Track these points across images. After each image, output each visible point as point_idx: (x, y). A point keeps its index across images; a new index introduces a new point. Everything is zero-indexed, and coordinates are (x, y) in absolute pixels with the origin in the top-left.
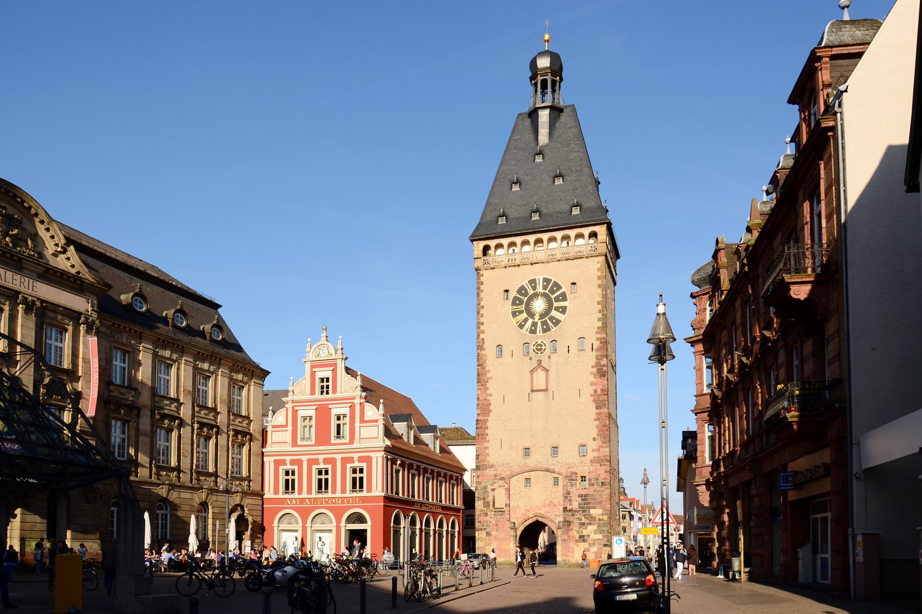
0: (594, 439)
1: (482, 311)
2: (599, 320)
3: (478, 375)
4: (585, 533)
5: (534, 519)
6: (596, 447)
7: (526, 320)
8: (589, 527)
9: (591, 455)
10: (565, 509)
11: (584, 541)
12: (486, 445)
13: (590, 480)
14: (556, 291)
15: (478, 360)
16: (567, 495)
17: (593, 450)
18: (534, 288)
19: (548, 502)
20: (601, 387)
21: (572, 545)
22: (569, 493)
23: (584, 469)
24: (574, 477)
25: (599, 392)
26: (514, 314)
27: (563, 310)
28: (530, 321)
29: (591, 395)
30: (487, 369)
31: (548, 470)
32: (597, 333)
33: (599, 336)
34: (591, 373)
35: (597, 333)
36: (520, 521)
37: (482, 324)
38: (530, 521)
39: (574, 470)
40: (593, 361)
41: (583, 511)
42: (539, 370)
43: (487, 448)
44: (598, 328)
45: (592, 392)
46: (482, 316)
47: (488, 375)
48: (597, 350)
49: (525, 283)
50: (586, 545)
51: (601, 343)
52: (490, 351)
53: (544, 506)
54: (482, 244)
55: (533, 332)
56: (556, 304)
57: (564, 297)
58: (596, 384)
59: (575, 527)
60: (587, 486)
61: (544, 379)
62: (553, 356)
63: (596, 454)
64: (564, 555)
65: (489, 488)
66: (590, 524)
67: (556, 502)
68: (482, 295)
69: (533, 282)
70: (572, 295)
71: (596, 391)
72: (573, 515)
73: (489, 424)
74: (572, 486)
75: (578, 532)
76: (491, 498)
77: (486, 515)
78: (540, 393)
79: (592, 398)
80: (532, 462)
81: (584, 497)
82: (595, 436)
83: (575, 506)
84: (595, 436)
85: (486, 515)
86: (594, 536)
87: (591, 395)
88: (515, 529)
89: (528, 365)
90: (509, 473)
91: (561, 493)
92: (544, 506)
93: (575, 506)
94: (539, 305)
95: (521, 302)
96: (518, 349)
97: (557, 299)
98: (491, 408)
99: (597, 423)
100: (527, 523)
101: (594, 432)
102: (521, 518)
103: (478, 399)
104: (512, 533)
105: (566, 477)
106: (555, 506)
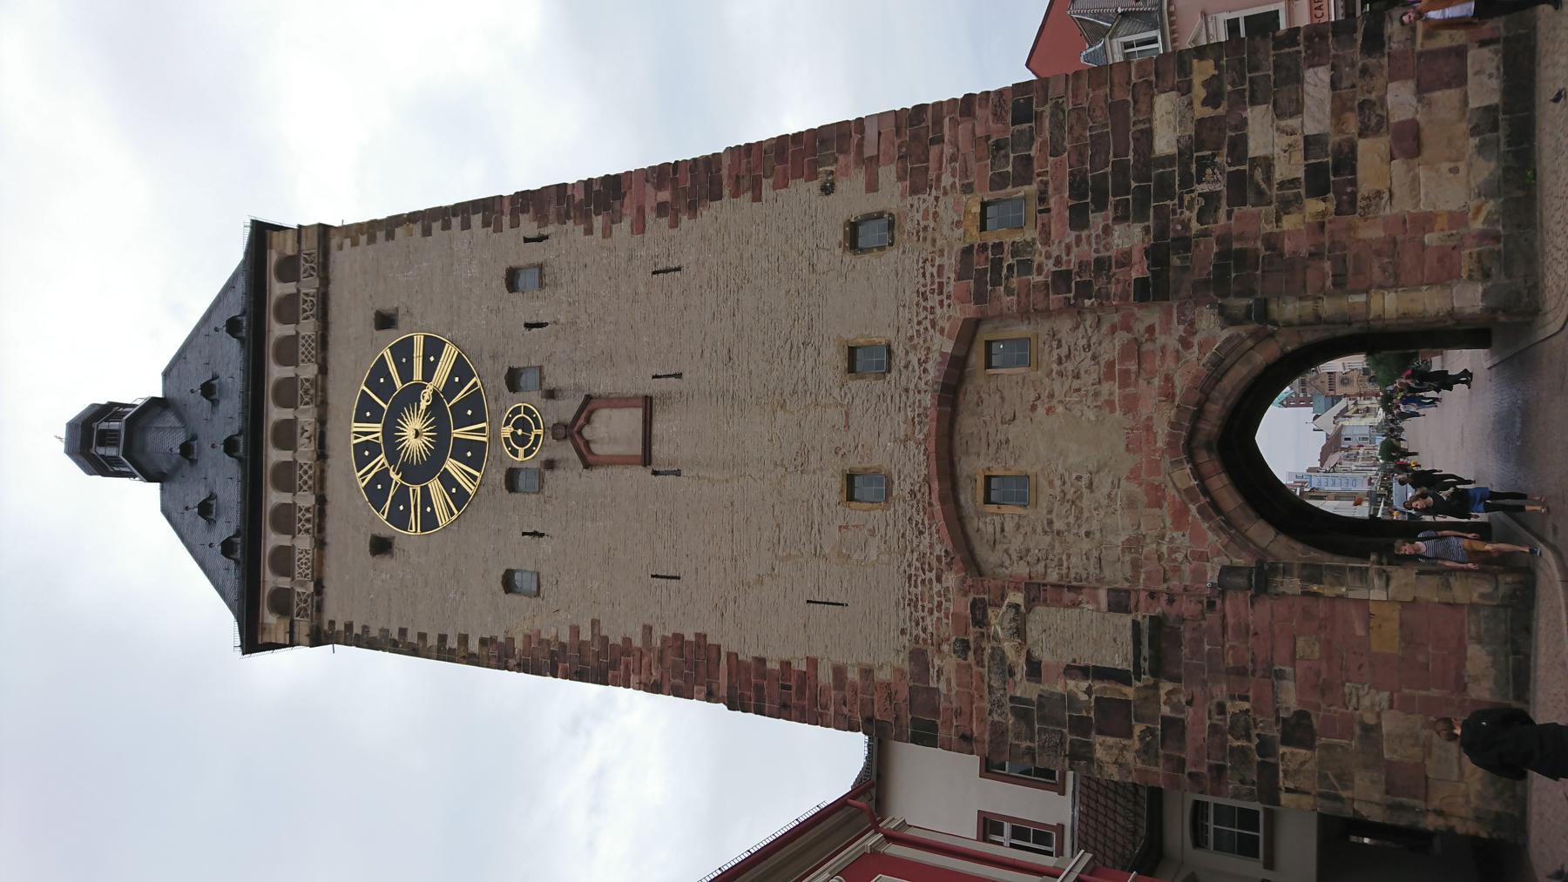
0: (827, 190)
1: (412, 638)
2: (466, 225)
3: (581, 676)
4: (1290, 167)
5: (1203, 457)
6: (860, 178)
7: (448, 481)
8: (1255, 148)
9: (891, 195)
10: (1149, 291)
11: (1346, 161)
12: (825, 676)
13: (999, 181)
14: (388, 376)
15: (537, 670)
16: (1077, 289)
17: (872, 186)
18: (374, 449)
19: (1111, 389)
20: (649, 188)
21: (1371, 232)
22: (1062, 278)
23: (949, 216)
24: (980, 263)
25: (665, 196)
26: (429, 521)
27: (434, 347)
28: (451, 465)
29: (675, 224)
30: (565, 638)
31: (951, 390)
32: (498, 229)
33: (506, 220)
34: (607, 233)
35: (498, 229)
36: (1213, 539)
37: (443, 638)
38: (1220, 483)
39: (951, 262)
40: (574, 229)
41: (1165, 189)
42: (587, 432)
43: (839, 672)
44: (486, 224)
45: (665, 221)
46: (422, 636)
47: (586, 635)
48: (542, 219)
49: (361, 479)
50: (1371, 152)
51: (524, 210)
52: (517, 620)
53: (1131, 404)
54: (269, 618)
55: (473, 454)
56: (418, 376)
57: (403, 351)
58: (641, 211)
59: (1253, 223)
60: (1032, 189)
61: (616, 413)
62: (550, 383)
63: (887, 173)
64: (1444, 276)
65: (1025, 689)
66: (1238, 147)
67: (1111, 349)
68: (374, 633)
69: (365, 452)
70: (403, 321)
71: (661, 209)
72: (1184, 243)
73: (748, 654)
74: (1026, 266)
75: (1286, 206)
76: (1078, 687)
77: (1174, 728)
78: (658, 428)
79: (685, 218)
80: (911, 466)
81: (1086, 197)
82: (815, 186)
83: (1130, 238)
84: (815, 186)
85: (1174, 728)
86: (1316, 117)
87: (675, 224)
88: (1262, 579)
89: (570, 478)
90: (951, 580)
91: (1064, 325)
92: (1131, 404)
93: (1130, 238)
94: (414, 435)
95: (402, 494)
96: (523, 510)
97: (406, 373)
98: (690, 636)
99: (766, 183)
100: (1231, 500)
101: (804, 191)
102: (1196, 551)
103: (655, 688)
104: (1292, 585)
105: (980, 297)
106: (1135, 351)
